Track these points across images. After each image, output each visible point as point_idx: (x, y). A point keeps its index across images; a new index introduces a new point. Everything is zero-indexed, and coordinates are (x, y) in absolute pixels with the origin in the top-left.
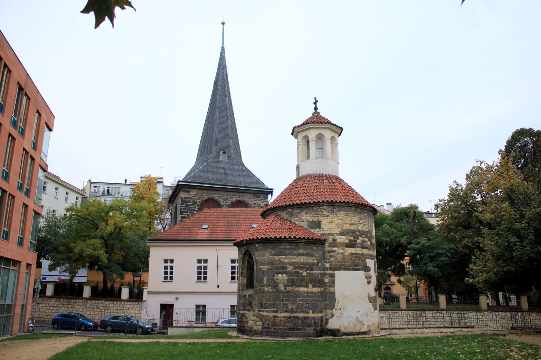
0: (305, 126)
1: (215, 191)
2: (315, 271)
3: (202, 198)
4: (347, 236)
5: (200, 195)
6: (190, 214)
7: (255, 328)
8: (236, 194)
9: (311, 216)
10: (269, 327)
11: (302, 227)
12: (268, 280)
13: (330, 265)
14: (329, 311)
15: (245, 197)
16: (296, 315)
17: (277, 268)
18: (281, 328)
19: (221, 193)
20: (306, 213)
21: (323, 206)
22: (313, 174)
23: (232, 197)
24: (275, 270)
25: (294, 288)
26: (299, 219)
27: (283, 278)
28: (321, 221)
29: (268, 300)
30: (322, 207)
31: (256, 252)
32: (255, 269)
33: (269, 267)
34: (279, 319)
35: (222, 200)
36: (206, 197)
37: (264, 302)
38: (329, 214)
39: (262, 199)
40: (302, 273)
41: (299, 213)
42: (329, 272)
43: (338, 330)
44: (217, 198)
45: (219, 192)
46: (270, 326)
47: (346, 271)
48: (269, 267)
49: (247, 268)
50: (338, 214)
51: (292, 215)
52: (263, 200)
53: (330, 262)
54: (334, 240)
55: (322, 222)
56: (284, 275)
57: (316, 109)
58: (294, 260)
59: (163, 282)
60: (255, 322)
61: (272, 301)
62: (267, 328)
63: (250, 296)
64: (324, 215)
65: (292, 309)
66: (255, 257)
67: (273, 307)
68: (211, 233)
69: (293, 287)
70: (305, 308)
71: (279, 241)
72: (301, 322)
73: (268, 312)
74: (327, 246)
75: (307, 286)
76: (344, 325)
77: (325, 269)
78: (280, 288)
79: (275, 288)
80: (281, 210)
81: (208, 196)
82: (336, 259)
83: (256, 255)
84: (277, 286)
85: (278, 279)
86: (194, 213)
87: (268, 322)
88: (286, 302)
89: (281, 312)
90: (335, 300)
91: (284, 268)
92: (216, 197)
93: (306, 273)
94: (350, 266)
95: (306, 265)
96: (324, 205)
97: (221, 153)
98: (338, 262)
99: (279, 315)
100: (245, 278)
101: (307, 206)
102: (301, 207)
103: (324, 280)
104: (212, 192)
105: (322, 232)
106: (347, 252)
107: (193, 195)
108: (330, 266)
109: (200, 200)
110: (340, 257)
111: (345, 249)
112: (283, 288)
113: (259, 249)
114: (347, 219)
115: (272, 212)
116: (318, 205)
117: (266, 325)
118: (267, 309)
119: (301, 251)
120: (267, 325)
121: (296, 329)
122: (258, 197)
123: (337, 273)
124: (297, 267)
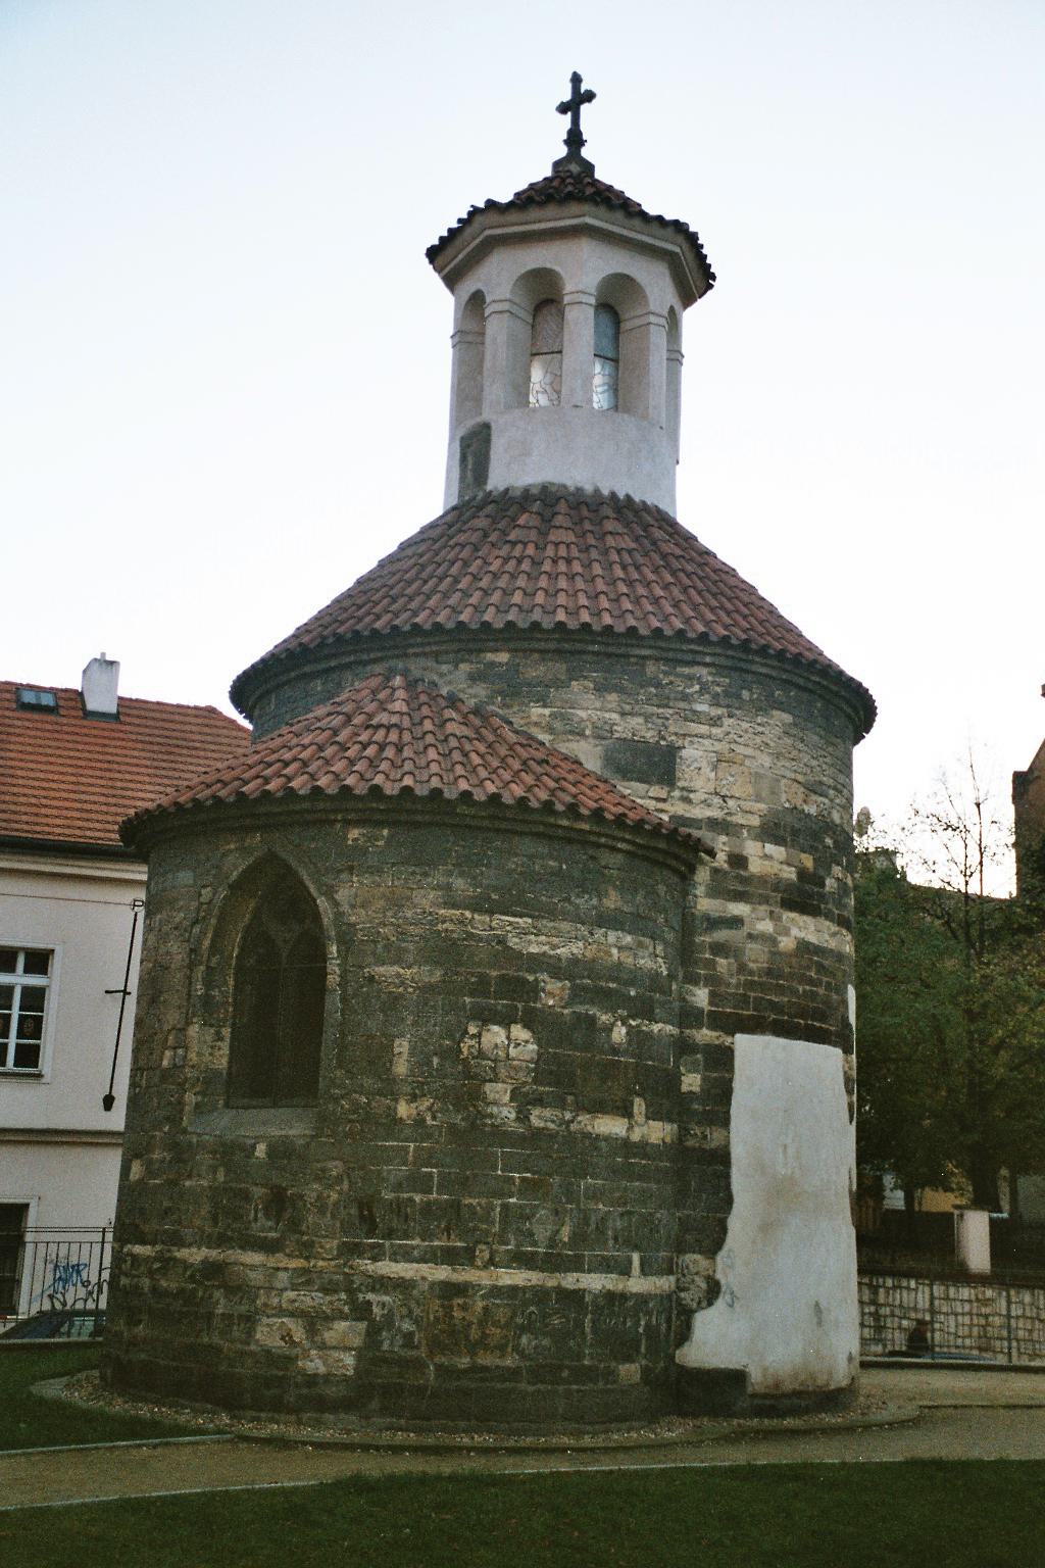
0: (534, 213)
2: (660, 1025)
4: (793, 846)
7: (315, 1364)
9: (628, 708)
11: (578, 762)
12: (420, 1058)
13: (713, 995)
14: (694, 1260)
16: (570, 1281)
17: (481, 987)
20: (601, 689)
22: (579, 490)
24: (467, 1000)
25: (568, 1116)
27: (513, 1052)
28: (680, 743)
32: (333, 979)
34: (480, 1304)
37: (388, 1196)
38: (720, 711)
40: (609, 1029)
42: (705, 1035)
43: (738, 1377)
46: (417, 1347)
47: (782, 1041)
50: (759, 720)
51: (514, 690)
53: (713, 981)
54: (738, 861)
55: (684, 753)
56: (519, 1032)
57: (575, 139)
58: (576, 948)
60: (314, 1321)
61: (441, 1189)
63: (281, 1151)
65: (552, 1242)
66: (336, 904)
67: (448, 1230)
69: (563, 1107)
70: (616, 1239)
72: (595, 1330)
73: (406, 1255)
74: (700, 891)
75: (627, 1112)
77: (688, 1016)
78: (495, 1110)
80: (436, 657)
82: (742, 968)
83: (342, 895)
84: (477, 1095)
85: (481, 1055)
87: (407, 1326)
88: (521, 1194)
93: (624, 1030)
95: (632, 983)
96: (698, 658)
98: (750, 985)
102: (572, 653)
105: (680, 809)
106: (787, 933)
108: (711, 1003)
110: (756, 956)
111: (779, 919)
112: (508, 1113)
113: (372, 861)
114: (795, 753)
116: (671, 655)
118: (407, 1237)
120: (399, 1341)
121: (565, 1374)
123: (743, 1043)
124: (584, 988)
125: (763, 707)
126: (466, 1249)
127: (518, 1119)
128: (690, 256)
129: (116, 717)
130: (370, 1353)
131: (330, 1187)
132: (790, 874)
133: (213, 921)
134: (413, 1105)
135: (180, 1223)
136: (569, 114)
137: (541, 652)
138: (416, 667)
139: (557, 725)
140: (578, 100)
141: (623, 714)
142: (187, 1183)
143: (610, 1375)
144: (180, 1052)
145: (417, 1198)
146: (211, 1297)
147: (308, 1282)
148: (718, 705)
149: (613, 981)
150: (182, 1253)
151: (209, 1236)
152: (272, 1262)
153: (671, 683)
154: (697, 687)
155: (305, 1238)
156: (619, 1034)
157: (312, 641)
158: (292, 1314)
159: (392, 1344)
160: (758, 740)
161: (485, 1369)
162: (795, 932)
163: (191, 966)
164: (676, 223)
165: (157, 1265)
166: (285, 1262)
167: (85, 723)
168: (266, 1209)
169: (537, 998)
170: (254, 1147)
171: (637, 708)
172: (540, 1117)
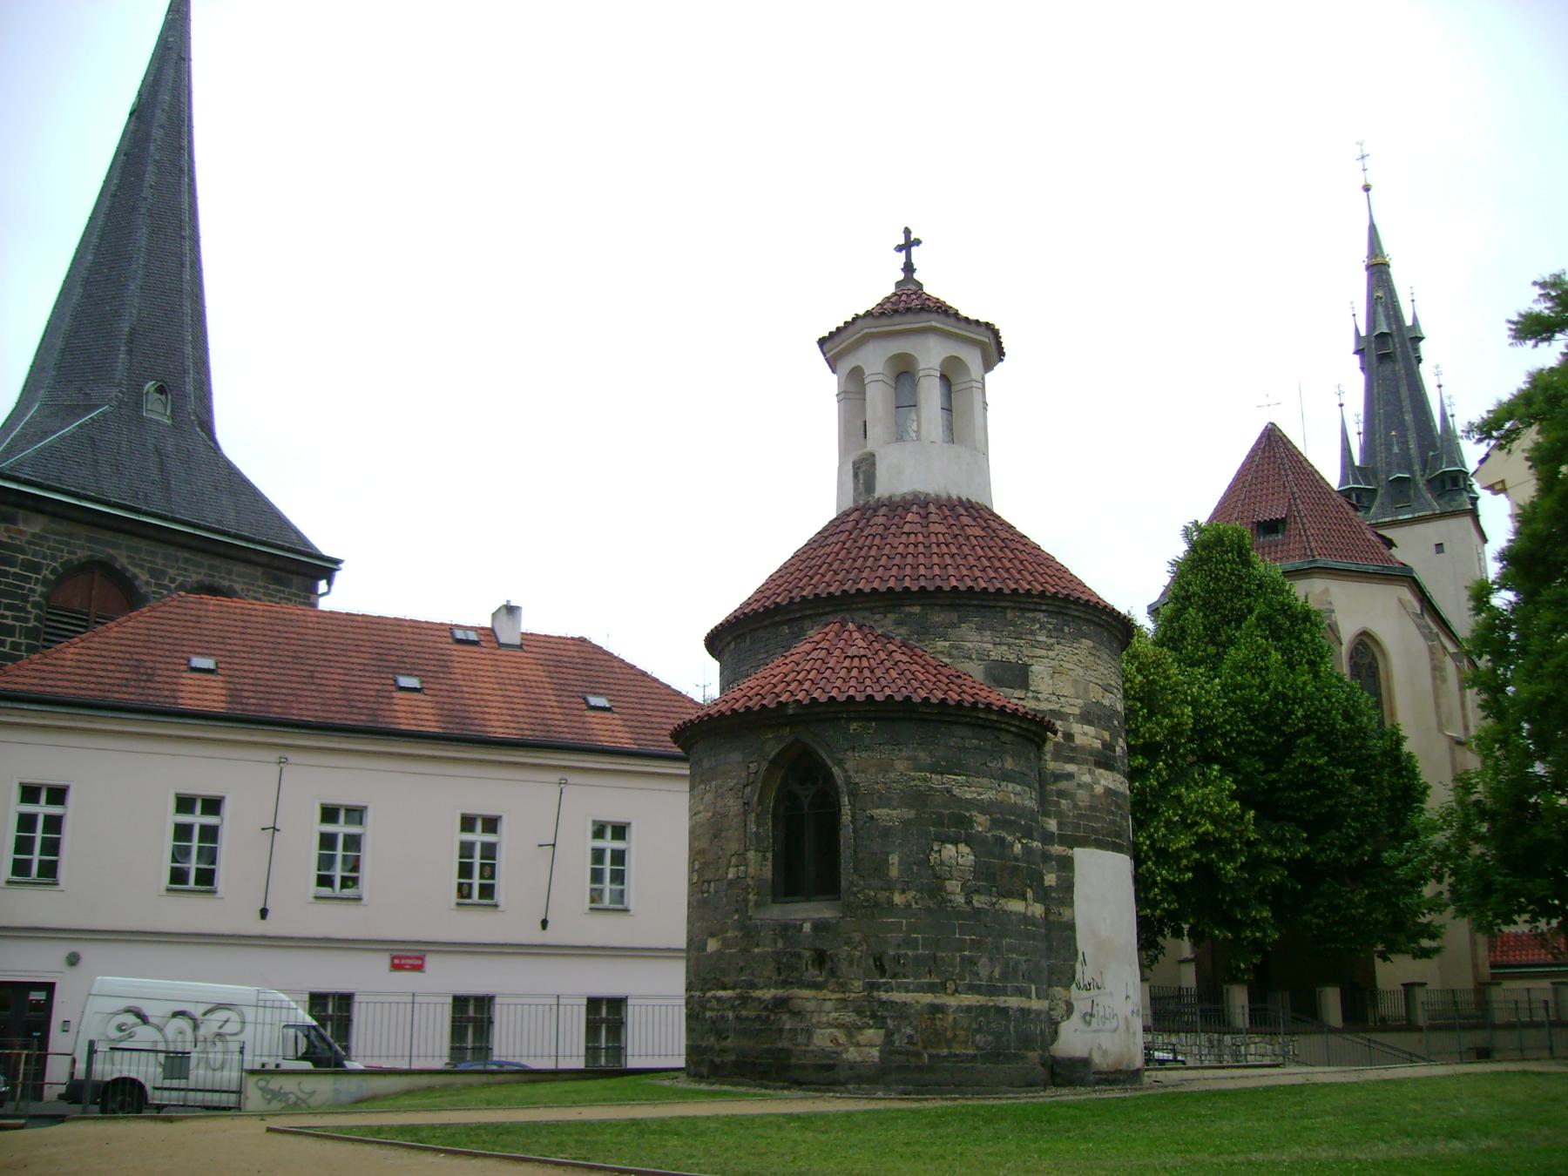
1: (121, 536)
3: (66, 556)
5: (55, 540)
6: (7, 613)
7: (852, 1054)
8: (198, 558)
10: (911, 1048)
13: (1060, 825)
15: (234, 577)
17: (939, 822)
18: (958, 1052)
19: (143, 544)
20: (979, 629)
21: (1035, 610)
23: (185, 570)
24: (932, 829)
25: (994, 900)
26: (951, 647)
27: (960, 861)
28: (1030, 662)
29: (908, 943)
30: (1030, 615)
31: (850, 753)
33: (912, 814)
34: (951, 1018)
35: (144, 577)
36: (81, 554)
37: (892, 953)
38: (1052, 641)
39: (295, 595)
40: (1012, 846)
41: (954, 626)
42: (1057, 849)
43: (1085, 1062)
44: (125, 561)
45: (134, 542)
46: (916, 1044)
48: (912, 814)
49: (774, 817)
50: (1075, 645)
51: (924, 631)
52: (299, 596)
53: (1059, 815)
54: (1069, 736)
56: (963, 848)
57: (909, 268)
59: (9, 882)
60: (851, 1030)
62: (907, 1053)
63: (819, 926)
64: (1036, 644)
65: (990, 978)
67: (930, 972)
68: (234, 695)
70: (1023, 976)
71: (947, 719)
74: (1048, 757)
75: (1024, 898)
76: (1100, 1047)
77: (1047, 838)
78: (953, 897)
79: (932, 896)
80: (872, 610)
81: (89, 549)
82: (1076, 806)
84: (941, 888)
85: (942, 863)
86: (23, 609)
87: (909, 1031)
89: (956, 991)
90: (1077, 951)
91: (964, 822)
92: (122, 560)
93: (1020, 846)
94: (1108, 835)
95: (1021, 816)
96: (1038, 607)
97: (150, 386)
98: (1080, 816)
99: (951, 1001)
100: (765, 858)
101: (985, 603)
103: (1043, 879)
104: (108, 536)
107: (28, 537)
108: (1059, 829)
109: (54, 559)
110: (1082, 797)
112: (960, 899)
115: (827, 610)
116: (1022, 606)
117: (898, 1041)
118: (905, 976)
119: (1009, 764)
122: (282, 584)
125: (1079, 635)
126: (941, 983)
127: (966, 903)
128: (993, 343)
129: (520, 647)
130: (887, 1045)
131: (855, 948)
132: (1098, 744)
133: (759, 785)
134: (904, 896)
135: (753, 974)
136: (904, 252)
137: (941, 606)
138: (858, 616)
139: (954, 652)
140: (908, 244)
141: (995, 644)
142: (756, 950)
143: (1024, 1058)
144: (742, 868)
145: (910, 953)
146: (780, 1018)
147: (845, 1007)
148: (1051, 637)
149: (1013, 815)
150: (758, 993)
151: (776, 982)
152: (821, 994)
153: (1022, 623)
154: (1038, 626)
155: (841, 980)
156: (1018, 847)
157: (783, 601)
158: (836, 1027)
159: (901, 1042)
160: (1075, 658)
161: (956, 1055)
162: (1103, 782)
163: (745, 813)
164: (987, 325)
165: (737, 1002)
166: (829, 995)
167: (498, 652)
168: (813, 964)
169: (972, 827)
170: (801, 925)
171: (1004, 640)
172: (978, 901)
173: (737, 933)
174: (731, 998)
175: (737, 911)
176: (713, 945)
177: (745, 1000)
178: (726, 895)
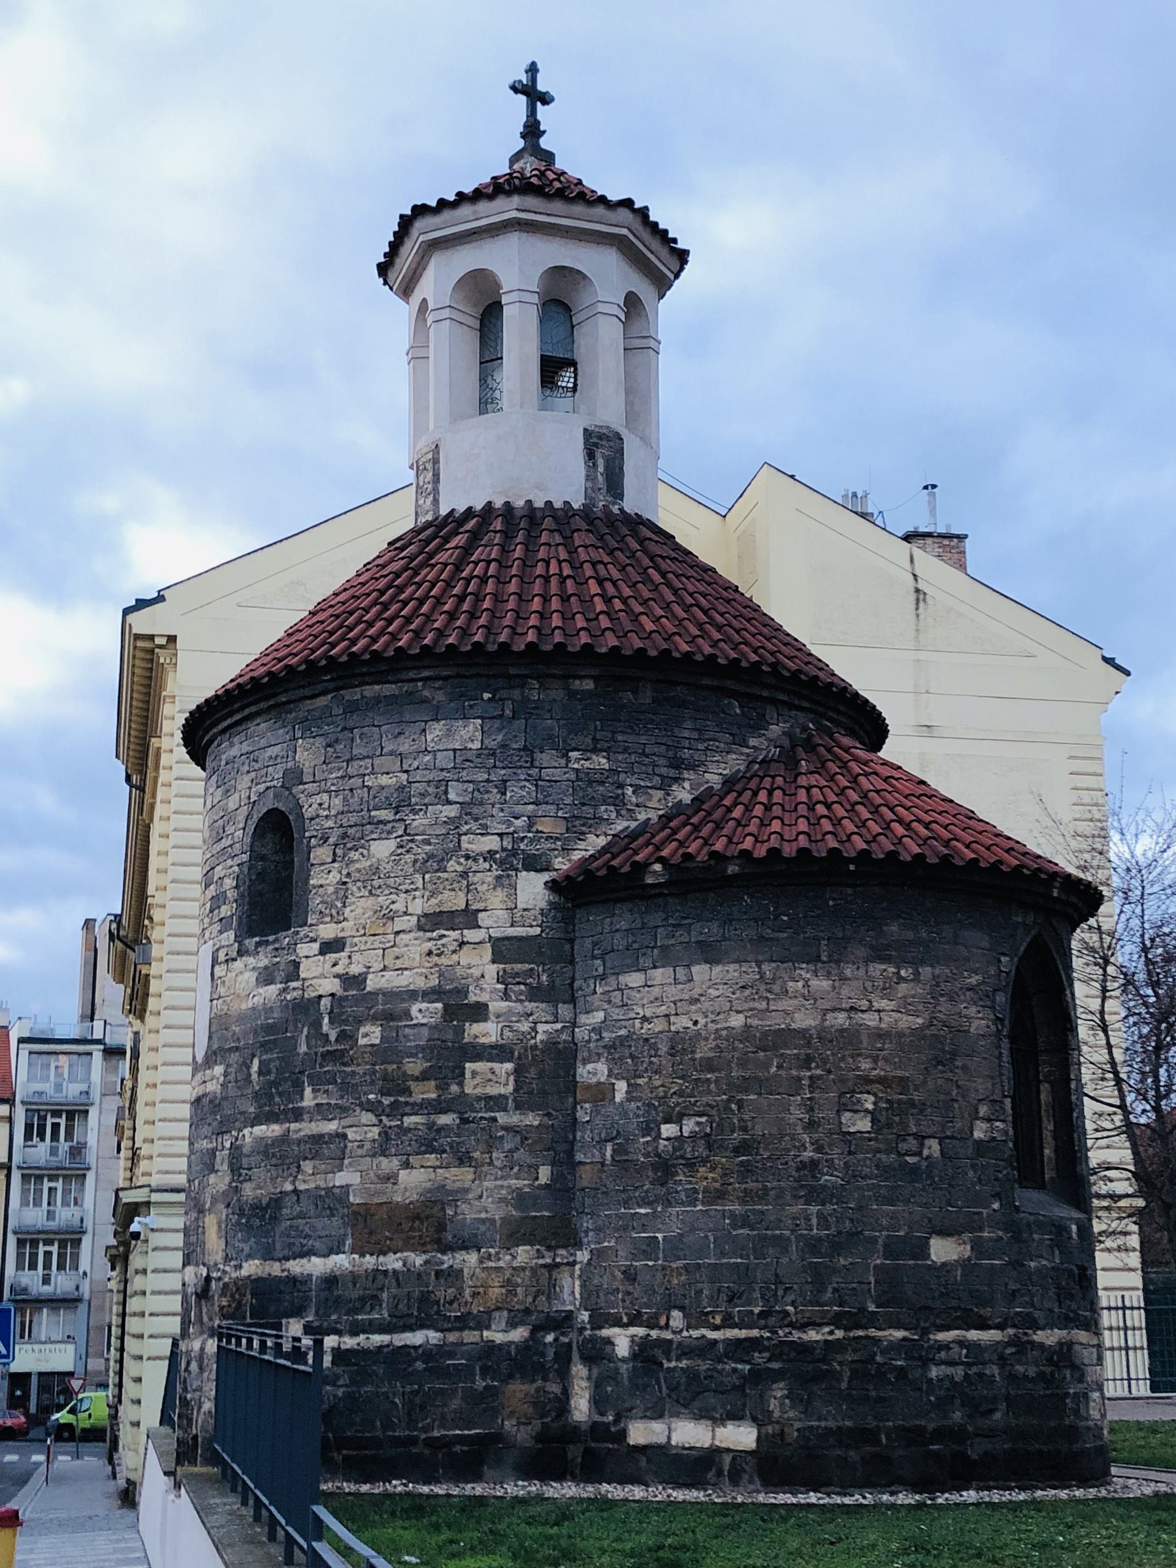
57: (532, 131)
135: (1033, 1306)
142: (1032, 1264)
150: (1040, 1336)
173: (1000, 1233)
174: (998, 1342)
175: (997, 1196)
176: (942, 1250)
177: (1021, 1346)
178: (973, 1166)
